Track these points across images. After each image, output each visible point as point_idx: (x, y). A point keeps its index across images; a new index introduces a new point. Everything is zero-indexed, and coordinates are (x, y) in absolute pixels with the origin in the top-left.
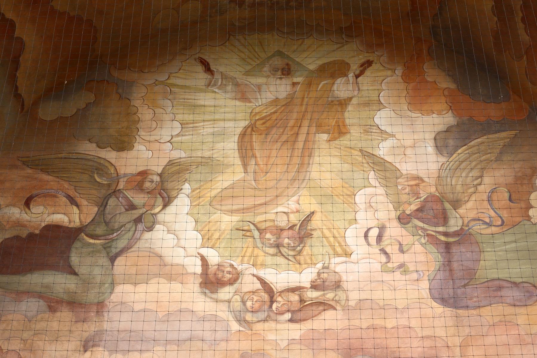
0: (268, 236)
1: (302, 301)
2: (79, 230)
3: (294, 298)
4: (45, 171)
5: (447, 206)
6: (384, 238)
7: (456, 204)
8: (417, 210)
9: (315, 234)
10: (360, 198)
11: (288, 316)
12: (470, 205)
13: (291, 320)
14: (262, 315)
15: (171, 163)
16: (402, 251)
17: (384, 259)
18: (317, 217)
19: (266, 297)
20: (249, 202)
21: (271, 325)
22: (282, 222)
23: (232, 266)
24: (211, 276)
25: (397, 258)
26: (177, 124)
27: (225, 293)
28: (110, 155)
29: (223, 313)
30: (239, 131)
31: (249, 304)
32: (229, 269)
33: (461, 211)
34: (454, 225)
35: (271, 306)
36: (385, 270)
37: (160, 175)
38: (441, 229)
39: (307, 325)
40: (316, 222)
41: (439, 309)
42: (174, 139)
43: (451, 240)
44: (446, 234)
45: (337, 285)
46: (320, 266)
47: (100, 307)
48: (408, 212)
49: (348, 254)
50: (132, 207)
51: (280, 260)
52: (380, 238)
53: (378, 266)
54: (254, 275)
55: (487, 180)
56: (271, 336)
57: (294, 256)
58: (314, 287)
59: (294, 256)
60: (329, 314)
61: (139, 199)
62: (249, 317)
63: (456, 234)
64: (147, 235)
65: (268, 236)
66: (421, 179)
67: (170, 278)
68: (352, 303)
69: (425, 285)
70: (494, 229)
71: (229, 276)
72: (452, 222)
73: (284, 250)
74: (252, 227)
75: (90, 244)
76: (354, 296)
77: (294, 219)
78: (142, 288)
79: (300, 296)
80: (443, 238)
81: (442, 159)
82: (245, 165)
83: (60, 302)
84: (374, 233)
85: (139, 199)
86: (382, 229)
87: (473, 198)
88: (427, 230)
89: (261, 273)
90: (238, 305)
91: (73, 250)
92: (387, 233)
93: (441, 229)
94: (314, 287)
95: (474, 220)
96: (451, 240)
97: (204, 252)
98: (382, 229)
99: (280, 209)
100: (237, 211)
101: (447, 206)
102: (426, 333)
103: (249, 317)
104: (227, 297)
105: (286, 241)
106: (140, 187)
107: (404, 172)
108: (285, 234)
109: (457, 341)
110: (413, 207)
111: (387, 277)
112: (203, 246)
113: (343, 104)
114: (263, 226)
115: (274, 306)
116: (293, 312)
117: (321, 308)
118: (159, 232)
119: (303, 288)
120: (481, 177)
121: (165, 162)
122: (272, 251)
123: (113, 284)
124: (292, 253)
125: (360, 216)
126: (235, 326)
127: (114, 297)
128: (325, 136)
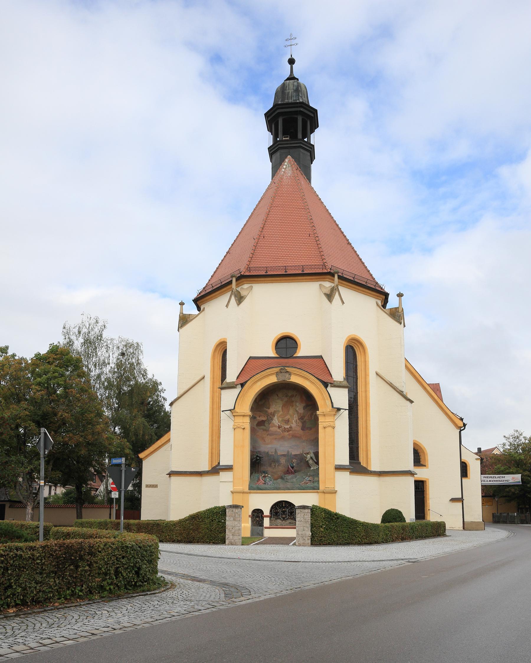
2: (265, 421)
7: (305, 417)
15: (274, 411)
22: (286, 419)
27: (281, 429)
28: (267, 410)
34: (304, 420)
41: (301, 431)
45: (292, 428)
50: (271, 417)
61: (271, 416)
82: (282, 411)
85: (271, 416)
106: (271, 415)
113: (293, 402)
118: (274, 420)
126: (282, 433)
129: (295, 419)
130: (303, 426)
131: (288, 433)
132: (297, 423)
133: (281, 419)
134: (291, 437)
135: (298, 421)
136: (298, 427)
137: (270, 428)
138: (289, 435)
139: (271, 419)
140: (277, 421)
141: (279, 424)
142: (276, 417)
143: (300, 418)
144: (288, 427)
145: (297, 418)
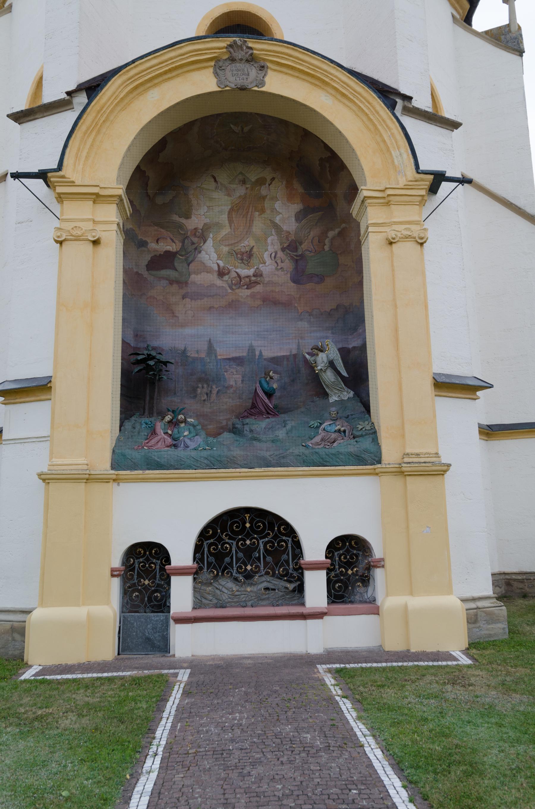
0: (239, 256)
1: (250, 281)
3: (248, 280)
4: (162, 227)
5: (298, 244)
6: (277, 256)
7: (301, 243)
8: (288, 246)
9: (254, 255)
10: (269, 240)
11: (246, 287)
12: (305, 244)
13: (247, 288)
14: (238, 286)
16: (282, 262)
17: (276, 265)
18: (255, 247)
19: (239, 279)
20: (233, 242)
21: (240, 290)
22: (243, 250)
23: (227, 267)
24: (221, 271)
25: (281, 265)
26: (206, 207)
27: (226, 278)
29: (225, 285)
30: (228, 210)
31: (233, 282)
32: (227, 269)
33: (302, 246)
35: (240, 283)
36: (277, 269)
37: (202, 230)
38: (295, 254)
39: (252, 290)
40: (255, 250)
41: (293, 284)
42: (206, 214)
43: (298, 258)
44: (296, 256)
45: (261, 275)
46: (256, 267)
47: (186, 283)
48: (285, 246)
49: (265, 263)
51: (242, 265)
52: (275, 257)
53: (274, 267)
54: (235, 271)
55: (311, 233)
56: (240, 294)
57: (247, 264)
58: (254, 276)
59: (247, 264)
60: (259, 285)
62: (234, 287)
63: (300, 256)
64: (199, 255)
65: (239, 256)
66: (290, 234)
67: (207, 272)
68: (265, 282)
69: (289, 275)
70: (312, 254)
71: (227, 271)
72: (299, 250)
73: (244, 261)
74: (234, 253)
75: (181, 259)
76: (267, 279)
77: (248, 249)
78: (199, 276)
79: (249, 279)
80: (295, 258)
81: (297, 224)
82: (231, 226)
83: (173, 281)
84: (273, 255)
86: (276, 253)
87: (307, 241)
88: (290, 254)
89: (237, 270)
90: (230, 282)
91: (175, 261)
92: (278, 255)
93: (295, 254)
94: (254, 276)
95: (306, 250)
96: (298, 258)
97: (218, 262)
98: (276, 253)
99: (242, 245)
100: (228, 245)
101: (298, 244)
102: (289, 293)
103: (234, 287)
104: (227, 279)
105: (245, 258)
107: (284, 230)
108: (245, 254)
109: (298, 296)
110: (286, 245)
111: (277, 273)
112: (218, 260)
114: (237, 252)
115: (242, 283)
116: (247, 285)
117: (256, 284)
119: (250, 276)
120: (310, 232)
121: (202, 225)
122: (240, 261)
123: (189, 275)
124: (246, 262)
125: (269, 247)
127: (190, 279)
128: (257, 213)
129: (271, 249)
130: (296, 268)
131: (248, 292)
132: (279, 261)
133: (225, 249)
134: (259, 302)
135: (280, 254)
136: (280, 273)
137: (193, 276)
138: (253, 296)
139: (196, 249)
140: (214, 256)
141: (221, 264)
142: (210, 242)
143: (285, 245)
144: (251, 272)
145: (277, 247)
